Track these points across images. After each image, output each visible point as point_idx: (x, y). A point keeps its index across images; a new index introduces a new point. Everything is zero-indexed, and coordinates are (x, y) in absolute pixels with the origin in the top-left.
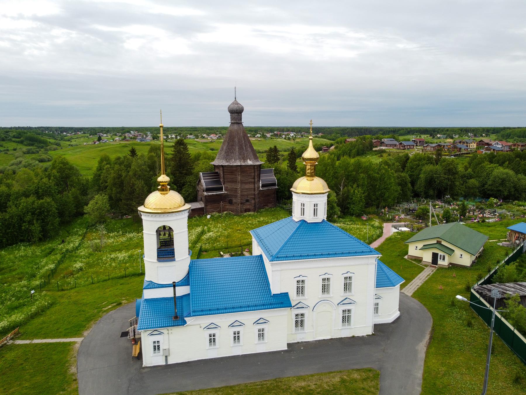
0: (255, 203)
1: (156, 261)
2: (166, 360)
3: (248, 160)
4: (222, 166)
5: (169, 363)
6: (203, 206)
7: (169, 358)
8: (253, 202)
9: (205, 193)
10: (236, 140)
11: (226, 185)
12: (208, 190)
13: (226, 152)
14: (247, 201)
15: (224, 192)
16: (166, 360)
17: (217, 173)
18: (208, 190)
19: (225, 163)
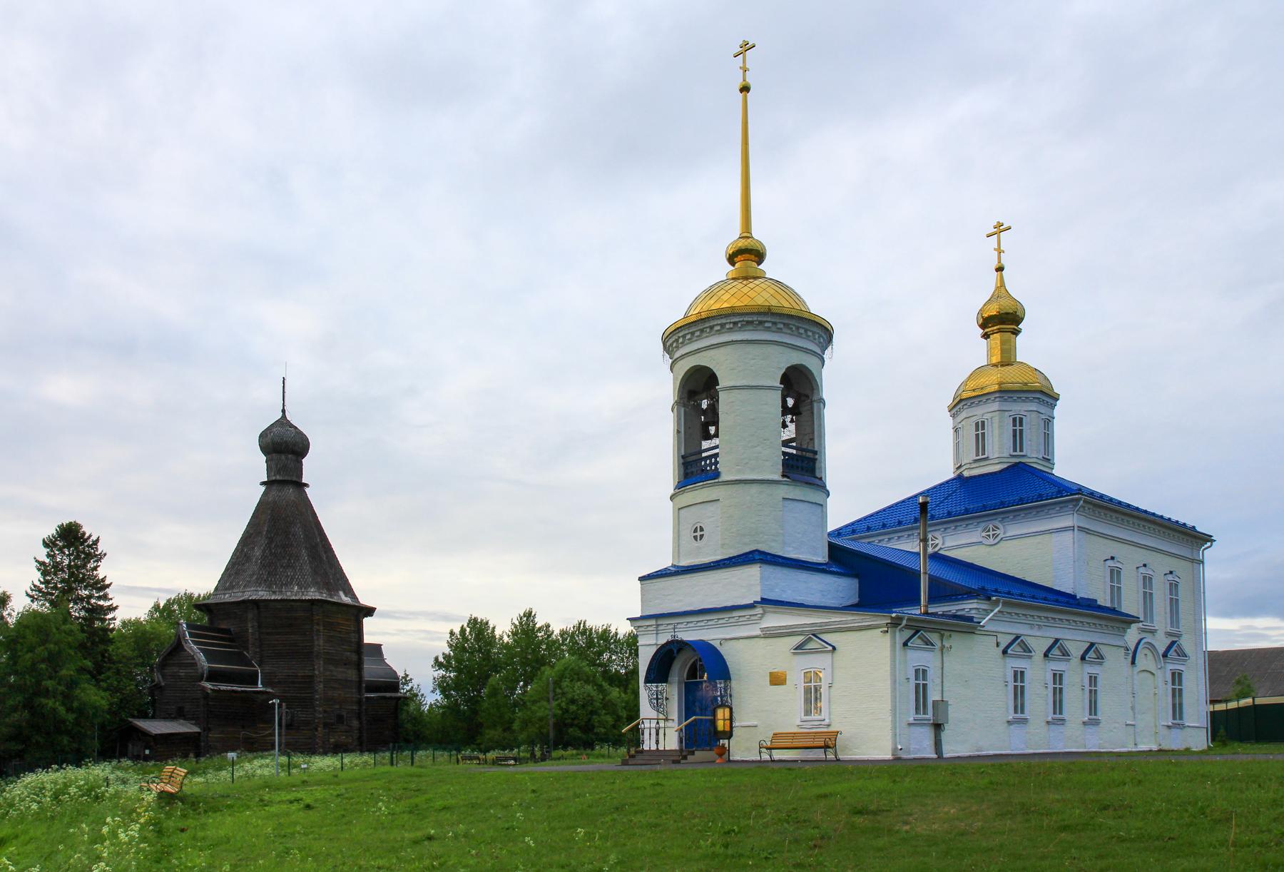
0: (360, 730)
1: (777, 477)
2: (938, 745)
3: (341, 593)
4: (256, 603)
5: (949, 751)
6: (197, 729)
7: (945, 736)
8: (355, 723)
9: (208, 685)
10: (298, 530)
11: (267, 668)
12: (214, 676)
13: (263, 566)
14: (340, 719)
15: (260, 687)
16: (938, 745)
17: (227, 631)
18: (214, 676)
19: (262, 594)
